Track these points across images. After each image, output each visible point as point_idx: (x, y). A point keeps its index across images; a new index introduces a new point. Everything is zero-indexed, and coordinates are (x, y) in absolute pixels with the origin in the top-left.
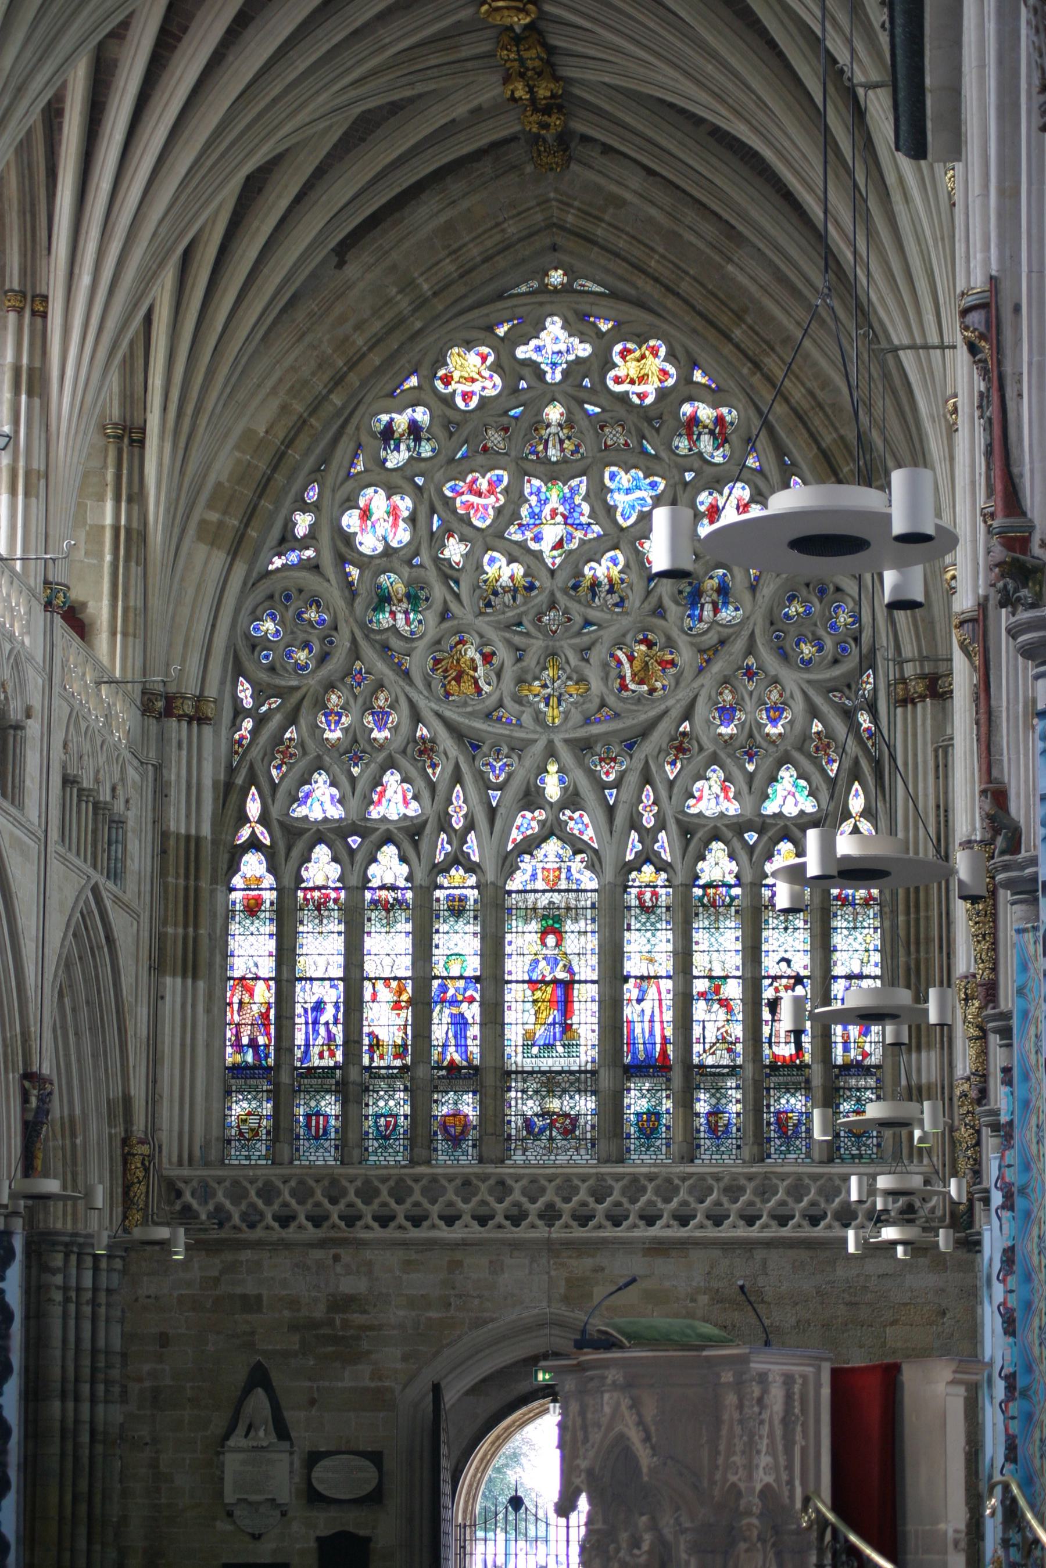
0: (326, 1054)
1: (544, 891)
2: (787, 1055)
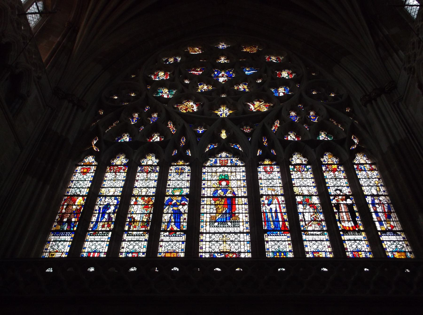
0: (106, 226)
1: (220, 166)
2: (350, 226)
